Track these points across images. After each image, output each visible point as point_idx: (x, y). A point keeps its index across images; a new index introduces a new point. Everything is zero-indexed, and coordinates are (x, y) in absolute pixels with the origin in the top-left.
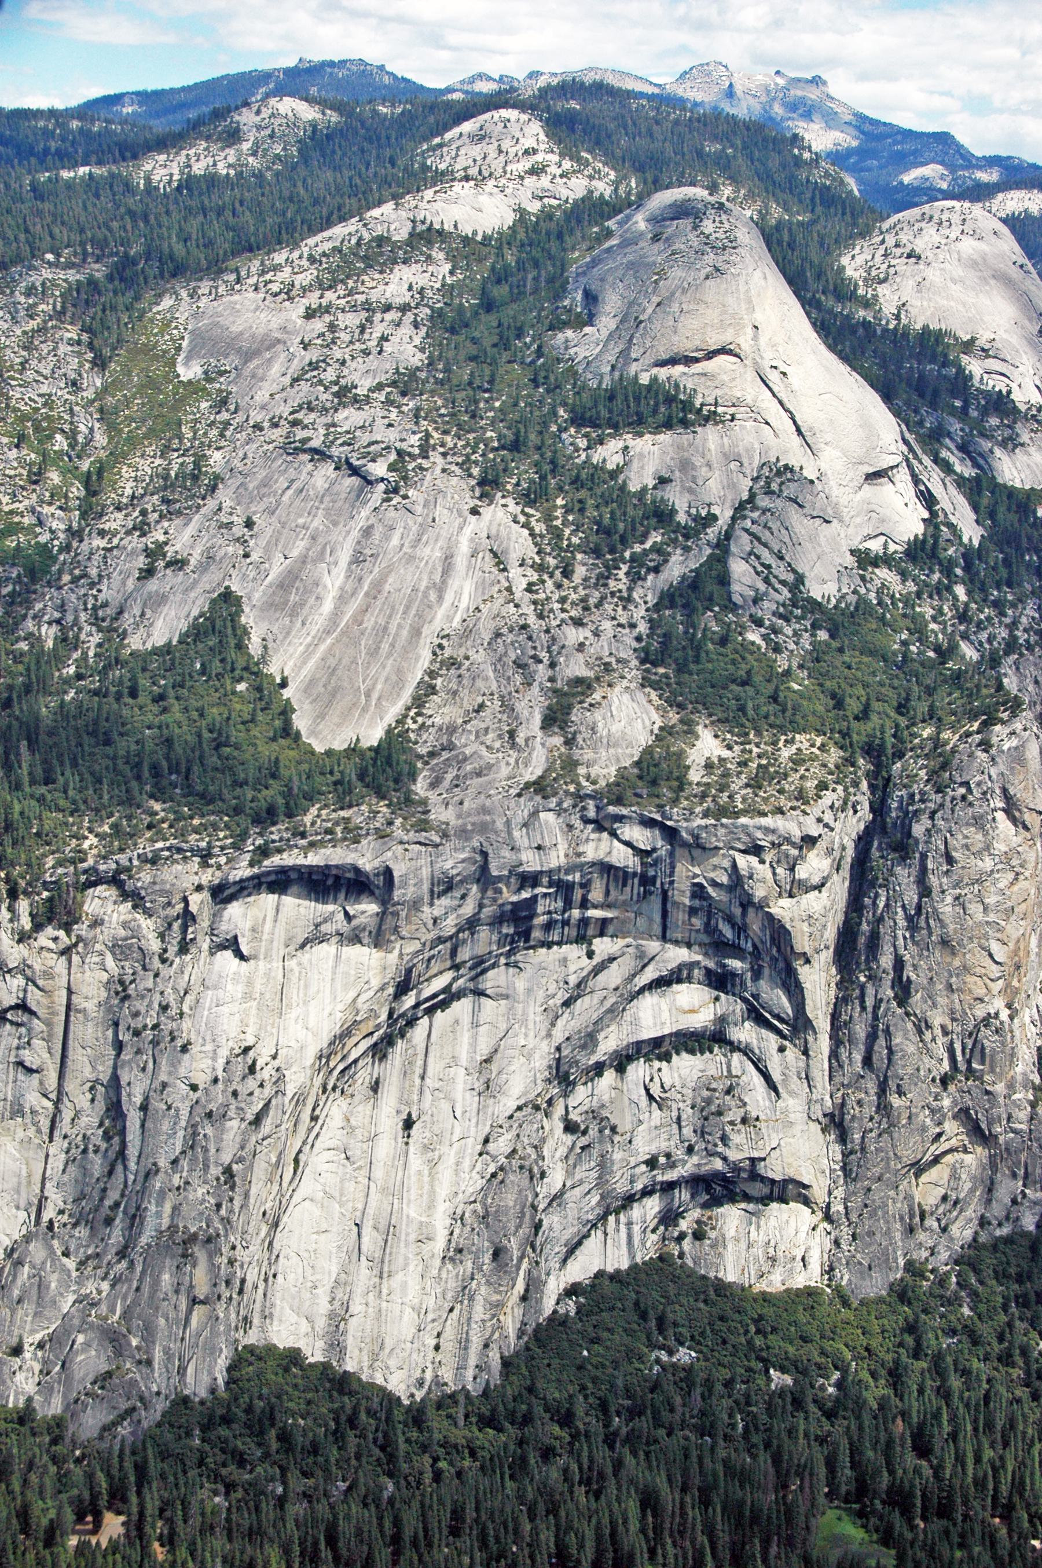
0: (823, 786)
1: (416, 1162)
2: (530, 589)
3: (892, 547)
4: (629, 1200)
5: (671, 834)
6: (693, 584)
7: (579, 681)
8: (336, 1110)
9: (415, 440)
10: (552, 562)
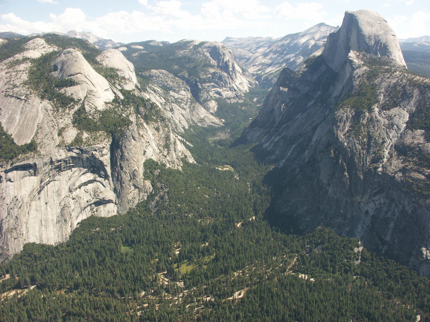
0: (105, 139)
1: (49, 209)
2: (52, 114)
3: (110, 101)
4: (85, 208)
5: (81, 150)
6: (79, 110)
7: (63, 128)
8: (34, 203)
9: (28, 92)
10: (55, 109)
